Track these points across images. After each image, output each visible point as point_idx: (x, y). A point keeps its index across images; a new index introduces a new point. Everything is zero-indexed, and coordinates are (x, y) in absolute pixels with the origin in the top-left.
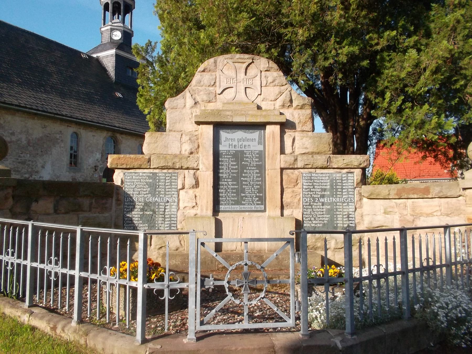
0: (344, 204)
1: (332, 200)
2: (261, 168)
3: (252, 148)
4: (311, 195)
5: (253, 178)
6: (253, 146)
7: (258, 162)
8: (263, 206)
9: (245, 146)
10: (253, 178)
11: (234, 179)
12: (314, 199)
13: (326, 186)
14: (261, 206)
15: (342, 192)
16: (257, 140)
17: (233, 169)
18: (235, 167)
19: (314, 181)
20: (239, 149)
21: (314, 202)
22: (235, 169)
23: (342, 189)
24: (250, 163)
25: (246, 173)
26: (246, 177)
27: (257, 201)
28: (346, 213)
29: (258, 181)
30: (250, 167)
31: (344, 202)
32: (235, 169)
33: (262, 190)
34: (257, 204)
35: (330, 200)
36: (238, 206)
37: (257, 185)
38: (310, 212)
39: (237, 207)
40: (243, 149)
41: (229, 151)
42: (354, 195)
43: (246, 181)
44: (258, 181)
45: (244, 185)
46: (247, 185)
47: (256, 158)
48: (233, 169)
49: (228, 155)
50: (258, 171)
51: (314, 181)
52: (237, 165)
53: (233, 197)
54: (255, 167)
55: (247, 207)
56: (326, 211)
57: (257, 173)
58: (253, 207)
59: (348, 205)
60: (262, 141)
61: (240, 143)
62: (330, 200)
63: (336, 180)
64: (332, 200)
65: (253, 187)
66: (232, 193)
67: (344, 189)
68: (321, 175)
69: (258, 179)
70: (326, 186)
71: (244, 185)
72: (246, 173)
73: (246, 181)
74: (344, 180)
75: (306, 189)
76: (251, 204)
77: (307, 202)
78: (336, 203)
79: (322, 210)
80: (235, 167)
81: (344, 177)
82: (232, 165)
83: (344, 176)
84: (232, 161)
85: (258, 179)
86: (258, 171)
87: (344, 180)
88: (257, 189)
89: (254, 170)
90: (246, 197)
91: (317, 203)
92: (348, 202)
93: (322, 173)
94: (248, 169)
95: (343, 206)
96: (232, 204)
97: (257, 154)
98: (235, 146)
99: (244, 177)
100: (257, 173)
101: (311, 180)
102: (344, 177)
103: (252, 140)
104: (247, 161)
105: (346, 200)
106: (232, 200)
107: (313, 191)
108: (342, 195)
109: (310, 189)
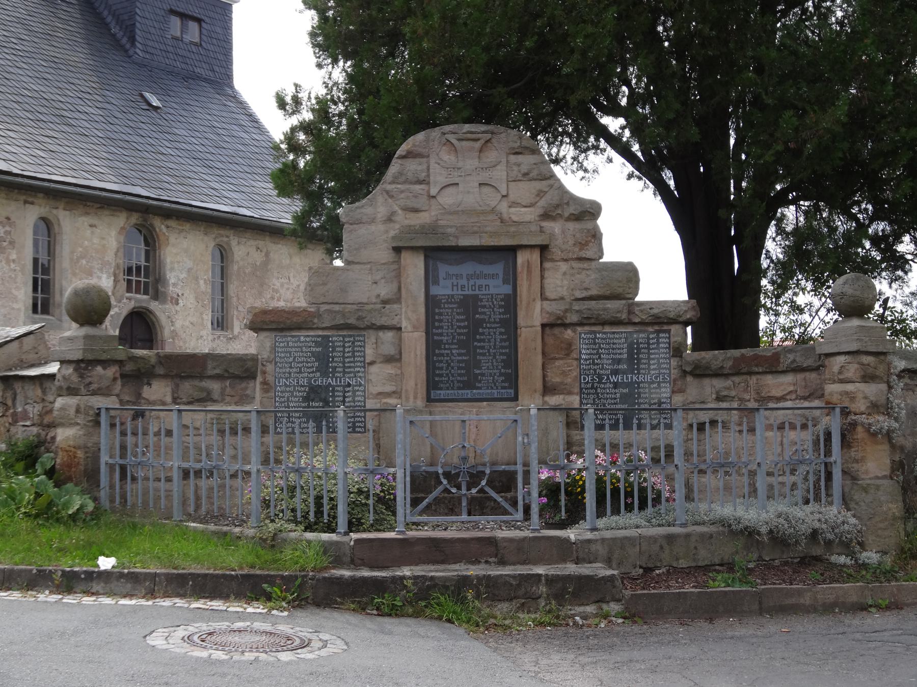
0: (652, 386)
1: (632, 378)
2: (511, 326)
3: (493, 291)
4: (595, 370)
5: (495, 343)
6: (494, 287)
7: (503, 314)
8: (512, 391)
9: (480, 287)
10: (495, 343)
11: (461, 344)
12: (600, 377)
13: (620, 354)
14: (509, 391)
15: (649, 364)
16: (501, 276)
17: (459, 327)
18: (462, 324)
19: (600, 347)
20: (471, 292)
21: (600, 382)
22: (464, 327)
23: (649, 359)
24: (490, 317)
25: (483, 334)
26: (483, 341)
27: (502, 381)
28: (656, 401)
29: (502, 347)
30: (490, 323)
31: (653, 382)
32: (464, 327)
33: (512, 363)
34: (503, 388)
35: (627, 378)
36: (469, 391)
37: (501, 354)
38: (594, 399)
39: (468, 393)
40: (477, 292)
41: (453, 296)
42: (670, 369)
43: (483, 348)
44: (502, 347)
45: (481, 354)
46: (484, 355)
47: (500, 307)
48: (459, 327)
49: (451, 303)
50: (503, 330)
51: (600, 347)
52: (467, 319)
53: (460, 375)
54: (497, 323)
55: (484, 392)
56: (621, 398)
57: (501, 333)
58: (495, 393)
59: (659, 387)
60: (512, 278)
61: (472, 282)
62: (627, 378)
63: (638, 343)
64: (632, 378)
65: (494, 357)
66: (459, 368)
67: (653, 359)
68: (612, 336)
69: (503, 344)
70: (620, 354)
71: (481, 354)
72: (483, 334)
73: (483, 348)
74: (653, 344)
75: (586, 360)
76: (492, 388)
77: (588, 382)
78: (638, 383)
79: (614, 396)
80: (462, 324)
81: (653, 339)
82: (458, 321)
83: (651, 336)
84: (458, 314)
85: (503, 344)
86: (503, 330)
87: (653, 344)
88: (503, 361)
89: (496, 328)
90: (483, 375)
91: (605, 383)
92: (659, 383)
93: (614, 333)
94: (487, 327)
95: (649, 387)
96: (459, 388)
97: (502, 300)
98: (463, 287)
99: (480, 341)
100: (501, 333)
101: (595, 344)
102: (653, 339)
103: (493, 276)
104: (484, 313)
105: (656, 378)
106: (458, 382)
107: (597, 364)
108: (649, 369)
109: (593, 360)
